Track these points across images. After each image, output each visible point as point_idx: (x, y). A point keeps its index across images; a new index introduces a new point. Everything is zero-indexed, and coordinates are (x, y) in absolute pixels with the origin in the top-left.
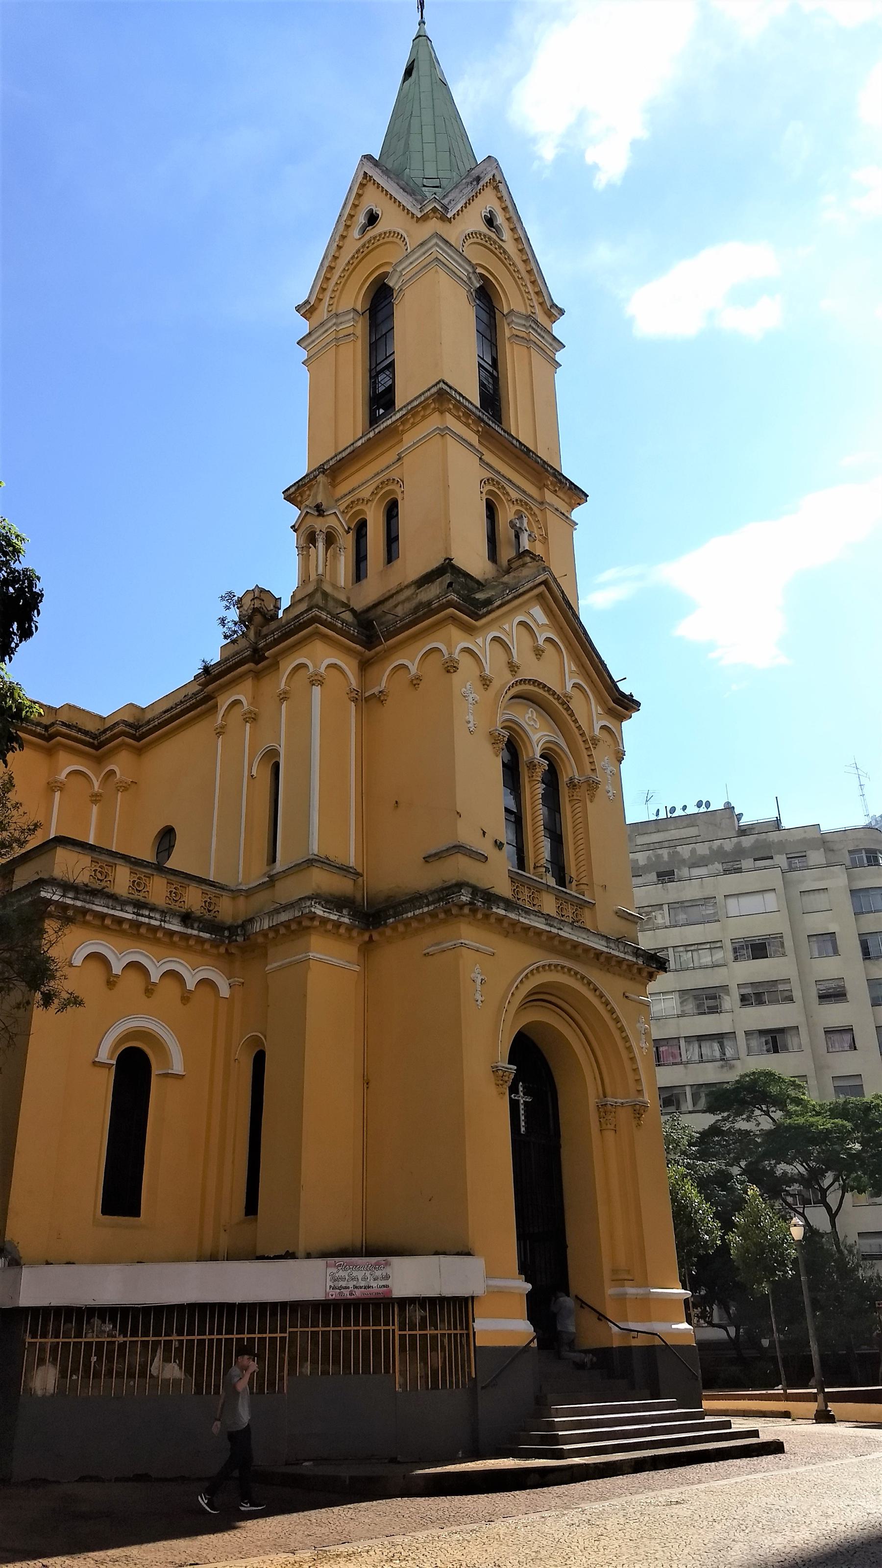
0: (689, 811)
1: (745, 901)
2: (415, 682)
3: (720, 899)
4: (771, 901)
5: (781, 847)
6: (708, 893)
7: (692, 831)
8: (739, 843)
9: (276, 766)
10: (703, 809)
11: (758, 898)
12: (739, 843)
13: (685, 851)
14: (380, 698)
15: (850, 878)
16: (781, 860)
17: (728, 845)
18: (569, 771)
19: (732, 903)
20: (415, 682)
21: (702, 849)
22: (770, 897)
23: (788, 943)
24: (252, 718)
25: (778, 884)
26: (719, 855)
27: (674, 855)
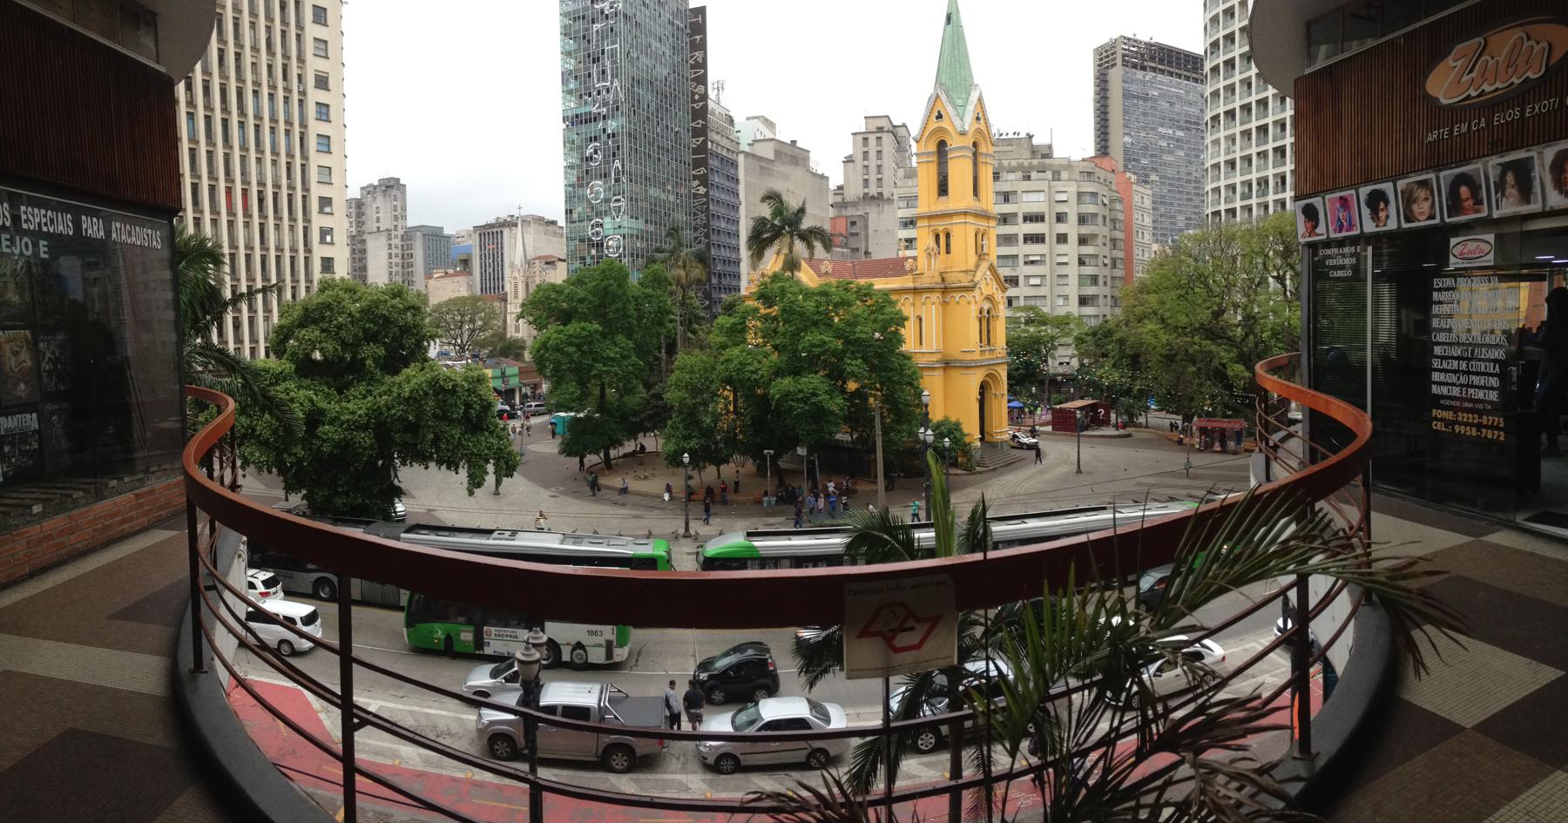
0: (1009, 137)
1: (1030, 194)
2: (958, 303)
3: (1019, 192)
4: (1042, 197)
5: (1050, 167)
6: (1013, 189)
7: (1010, 148)
8: (1031, 163)
9: (921, 320)
10: (1016, 136)
11: (1036, 194)
12: (1031, 163)
13: (1005, 163)
14: (947, 303)
15: (1078, 187)
16: (1049, 175)
17: (1026, 163)
18: (993, 313)
19: (1025, 195)
20: (958, 303)
21: (1014, 163)
22: (1042, 194)
23: (1047, 218)
24: (913, 304)
25: (1046, 189)
26: (1020, 168)
27: (1000, 164)
